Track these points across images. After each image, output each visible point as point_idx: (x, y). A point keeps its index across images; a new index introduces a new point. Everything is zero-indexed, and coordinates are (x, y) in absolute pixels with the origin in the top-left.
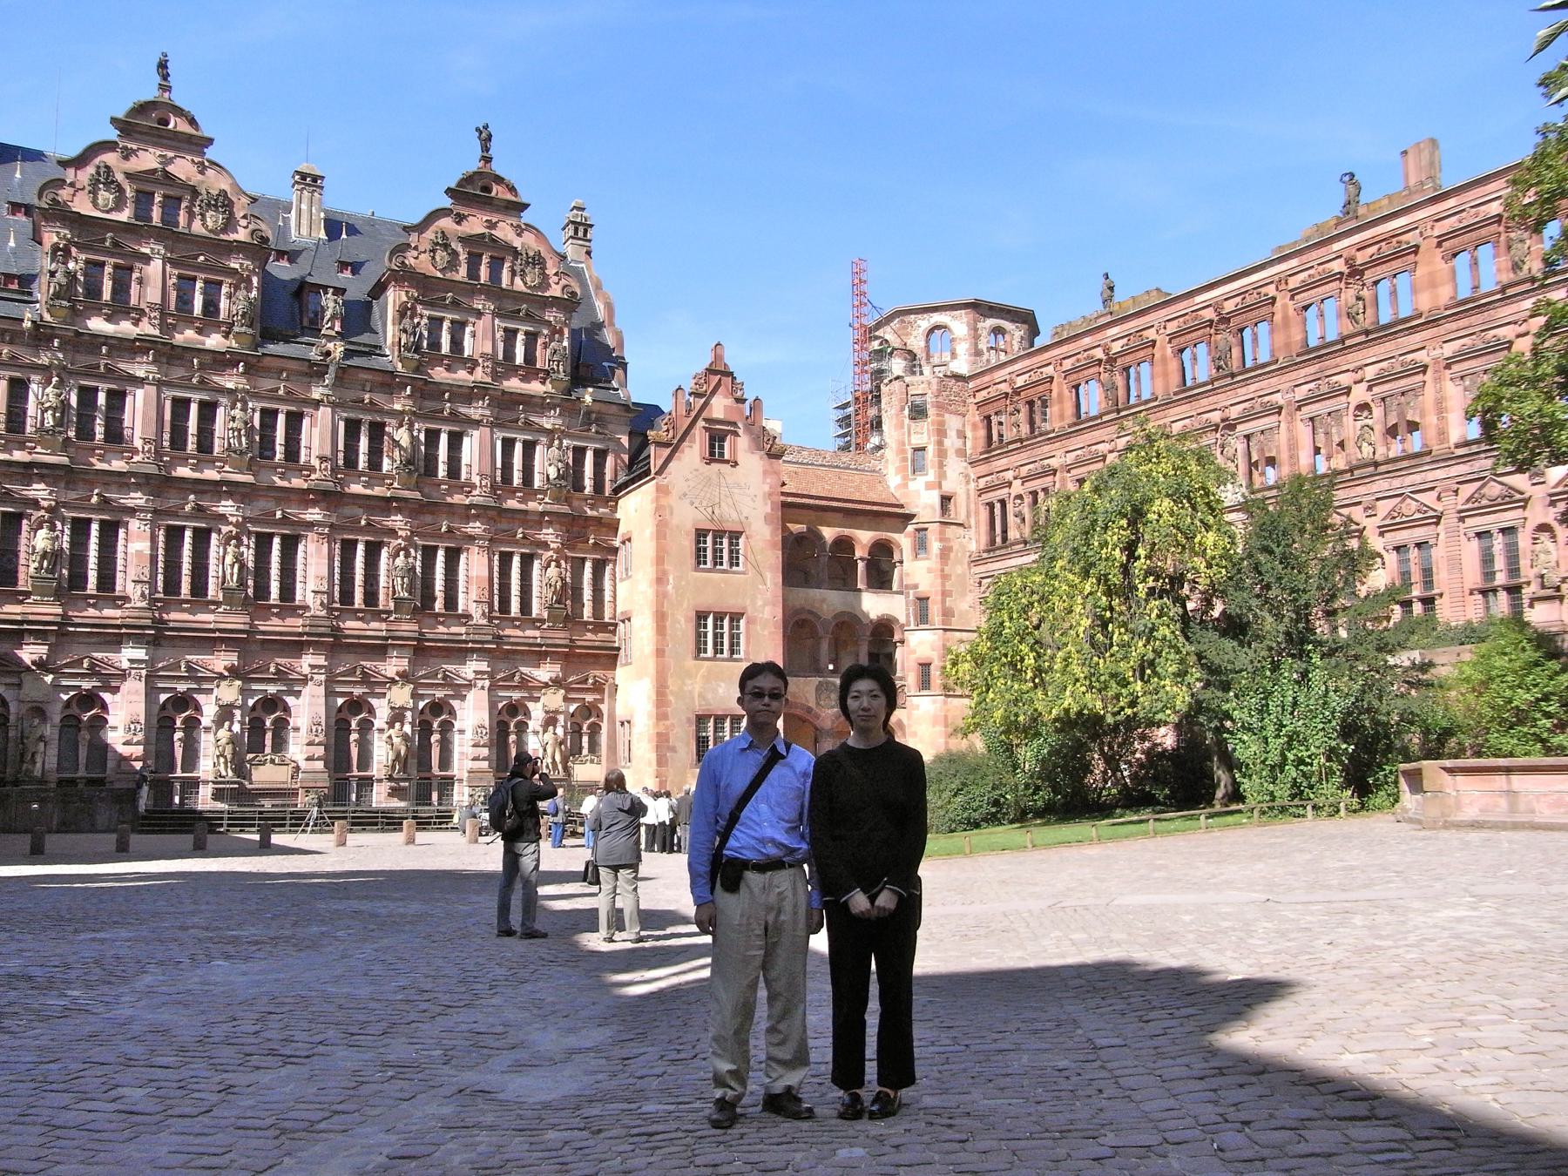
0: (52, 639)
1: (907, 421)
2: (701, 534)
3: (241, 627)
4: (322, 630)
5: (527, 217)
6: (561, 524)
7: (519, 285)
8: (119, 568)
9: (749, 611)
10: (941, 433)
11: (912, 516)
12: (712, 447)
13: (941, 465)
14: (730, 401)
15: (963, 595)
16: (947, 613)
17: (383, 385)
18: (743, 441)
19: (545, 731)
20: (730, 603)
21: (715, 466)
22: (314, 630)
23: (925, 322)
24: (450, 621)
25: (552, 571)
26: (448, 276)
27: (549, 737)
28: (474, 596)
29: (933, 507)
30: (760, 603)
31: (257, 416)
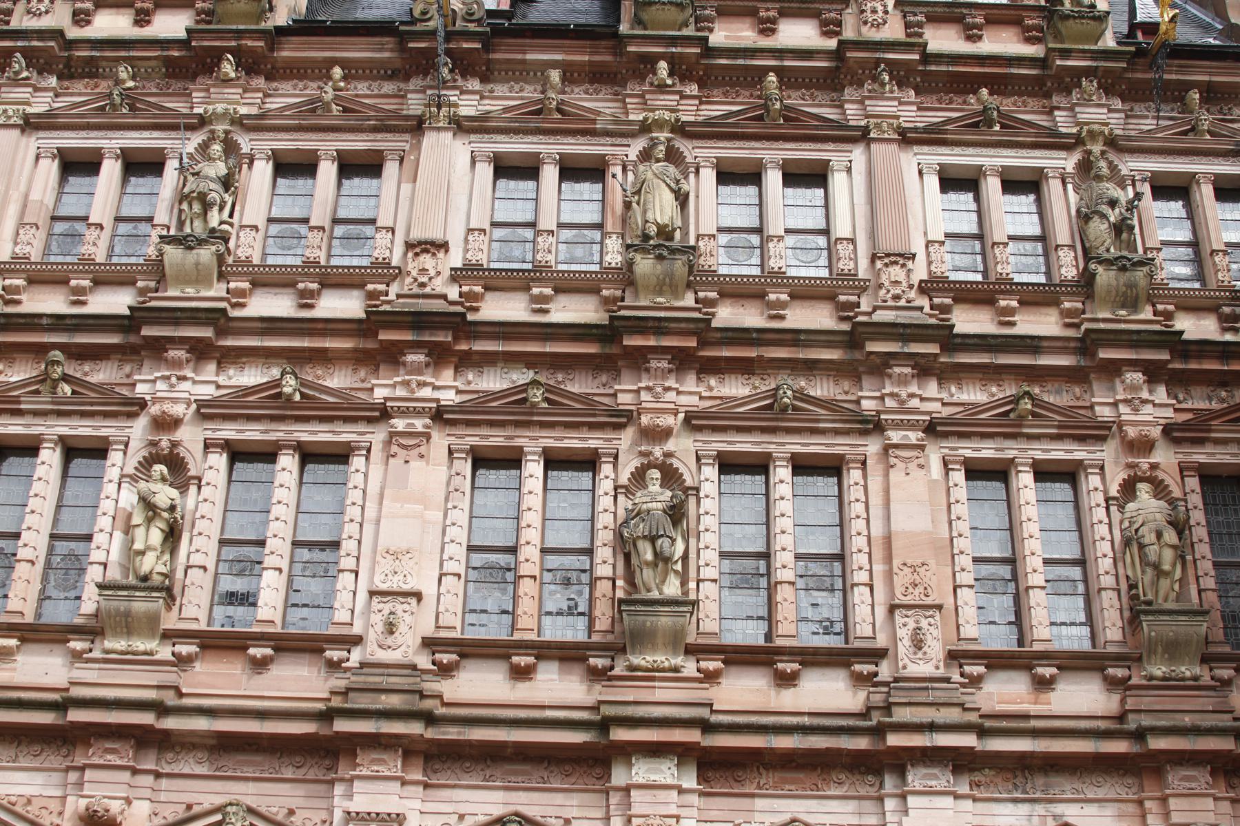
4: (394, 701)
6: (1154, 374)
17: (598, 77)
25: (1146, 502)
31: (263, 170)
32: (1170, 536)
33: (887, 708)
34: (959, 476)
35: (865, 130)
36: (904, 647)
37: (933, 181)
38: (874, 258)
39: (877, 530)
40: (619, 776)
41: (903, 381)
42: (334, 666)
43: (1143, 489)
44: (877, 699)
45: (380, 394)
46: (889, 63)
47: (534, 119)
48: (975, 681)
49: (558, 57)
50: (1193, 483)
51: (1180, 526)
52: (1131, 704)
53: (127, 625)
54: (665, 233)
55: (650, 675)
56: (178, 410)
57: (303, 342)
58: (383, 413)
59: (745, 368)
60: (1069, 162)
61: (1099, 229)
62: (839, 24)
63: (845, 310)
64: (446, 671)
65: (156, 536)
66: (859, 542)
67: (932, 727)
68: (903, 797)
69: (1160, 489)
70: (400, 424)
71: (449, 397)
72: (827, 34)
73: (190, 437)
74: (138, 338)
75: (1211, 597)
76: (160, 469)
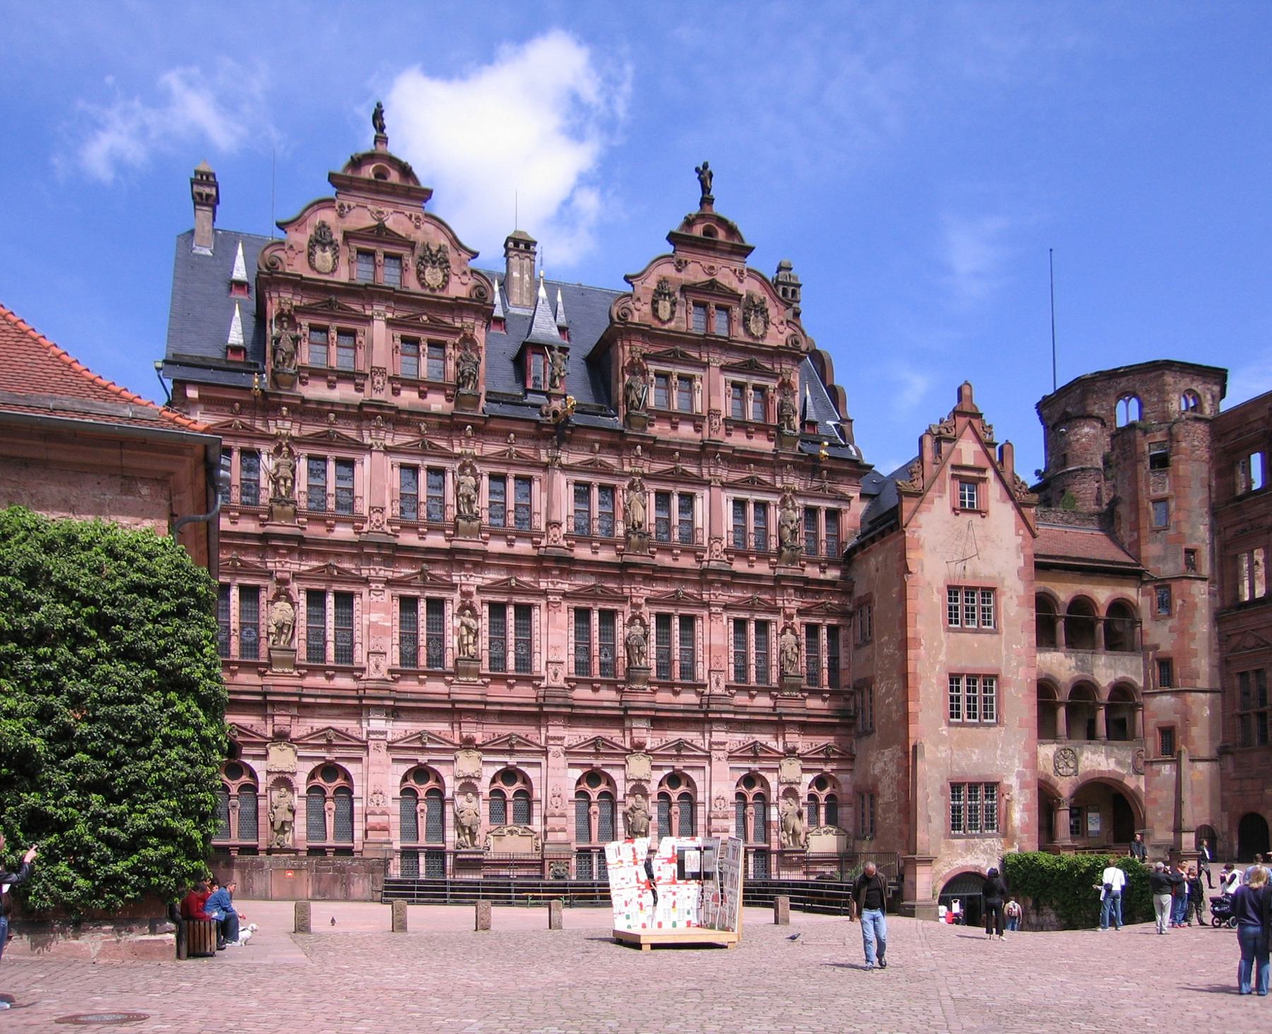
0: (295, 712)
2: (953, 590)
3: (479, 698)
4: (560, 701)
5: (751, 261)
8: (357, 640)
12: (963, 497)
18: (993, 489)
22: (549, 701)
26: (672, 325)
31: (485, 482)
33: (708, 704)
34: (732, 624)
35: (710, 482)
36: (714, 684)
37: (731, 504)
38: (710, 539)
39: (707, 642)
40: (627, 724)
41: (717, 589)
42: (537, 687)
44: (705, 701)
45: (543, 585)
47: (592, 467)
48: (733, 695)
49: (598, 438)
53: (467, 672)
55: (637, 691)
56: (473, 589)
57: (512, 562)
58: (544, 593)
59: (665, 580)
60: (778, 500)
61: (787, 531)
63: (699, 560)
64: (572, 688)
65: (471, 638)
66: (700, 646)
67: (721, 712)
70: (551, 598)
71: (566, 587)
72: (697, 431)
73: (477, 599)
74: (454, 558)
76: (468, 612)
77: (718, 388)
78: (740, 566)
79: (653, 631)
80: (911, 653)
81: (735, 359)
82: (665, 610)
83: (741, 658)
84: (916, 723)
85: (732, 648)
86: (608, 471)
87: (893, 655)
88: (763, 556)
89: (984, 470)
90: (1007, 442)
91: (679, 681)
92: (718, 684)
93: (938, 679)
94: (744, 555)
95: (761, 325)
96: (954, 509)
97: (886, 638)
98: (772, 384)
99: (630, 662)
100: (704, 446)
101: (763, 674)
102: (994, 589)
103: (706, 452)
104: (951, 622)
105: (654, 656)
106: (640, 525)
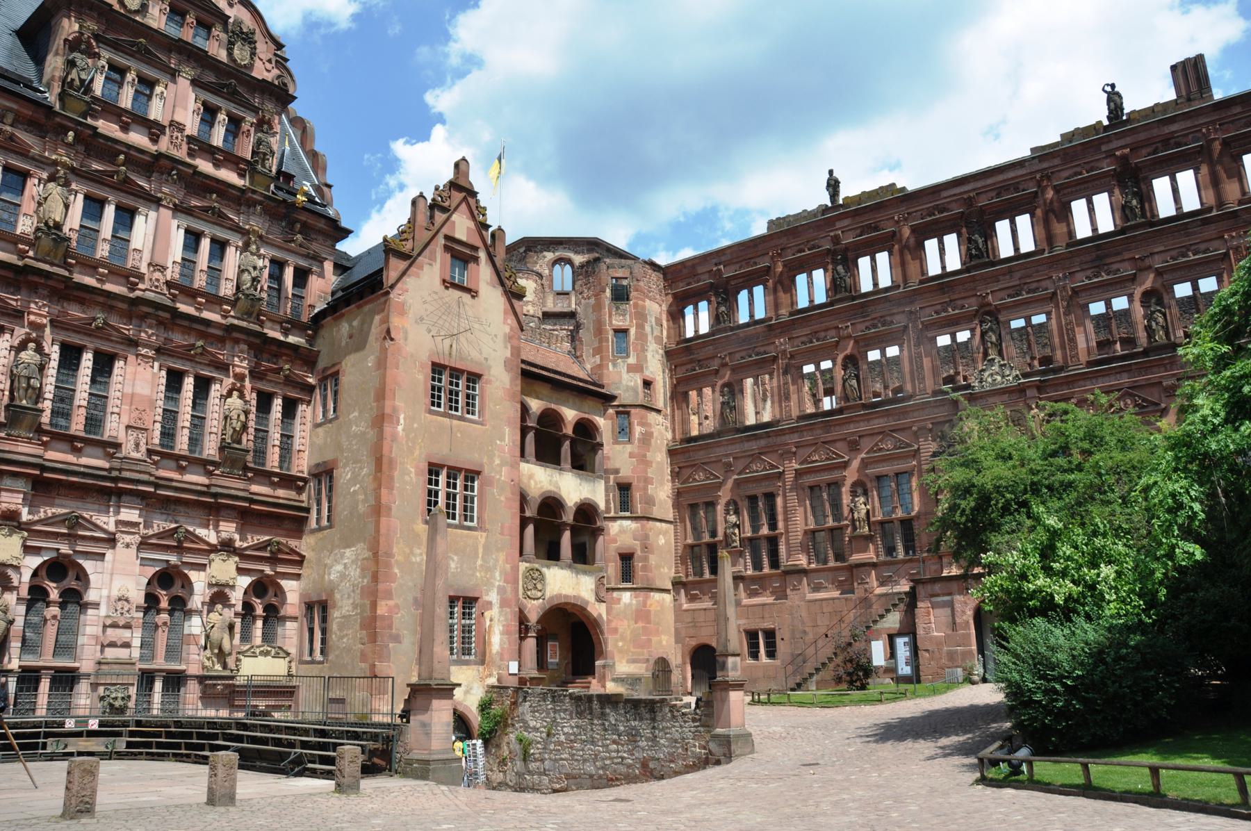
1: (607, 302)
2: (437, 368)
7: (223, 55)
9: (486, 471)
10: (641, 316)
11: (613, 398)
13: (644, 350)
14: (471, 224)
15: (662, 484)
16: (650, 501)
19: (209, 612)
20: (466, 458)
21: (456, 294)
23: (550, 256)
24: (88, 450)
25: (235, 401)
27: (214, 617)
28: (125, 420)
29: (635, 390)
30: (497, 462)
32: (243, 418)
34: (164, 373)
35: (160, 199)
37: (182, 232)
38: (150, 264)
43: (235, 393)
44: (116, 464)
46: (178, 170)
50: (254, 395)
51: (247, 413)
52: (214, 481)
54: (58, 226)
59: (82, 302)
62: (158, 137)
68: (119, 507)
69: (242, 396)
75: (251, 444)
77: (186, 98)
78: (183, 308)
79: (54, 364)
80: (387, 429)
81: (210, 78)
82: (76, 339)
83: (170, 416)
84: (389, 515)
85: (160, 403)
86: (24, 154)
87: (364, 433)
88: (215, 300)
89: (476, 249)
90: (500, 229)
91: (83, 434)
92: (137, 445)
93: (417, 467)
94: (192, 294)
95: (247, 54)
96: (444, 281)
97: (356, 414)
98: (250, 119)
99: (12, 397)
100: (160, 156)
101: (195, 441)
102: (479, 376)
103: (157, 164)
104: (433, 404)
105: (49, 396)
106: (58, 226)
